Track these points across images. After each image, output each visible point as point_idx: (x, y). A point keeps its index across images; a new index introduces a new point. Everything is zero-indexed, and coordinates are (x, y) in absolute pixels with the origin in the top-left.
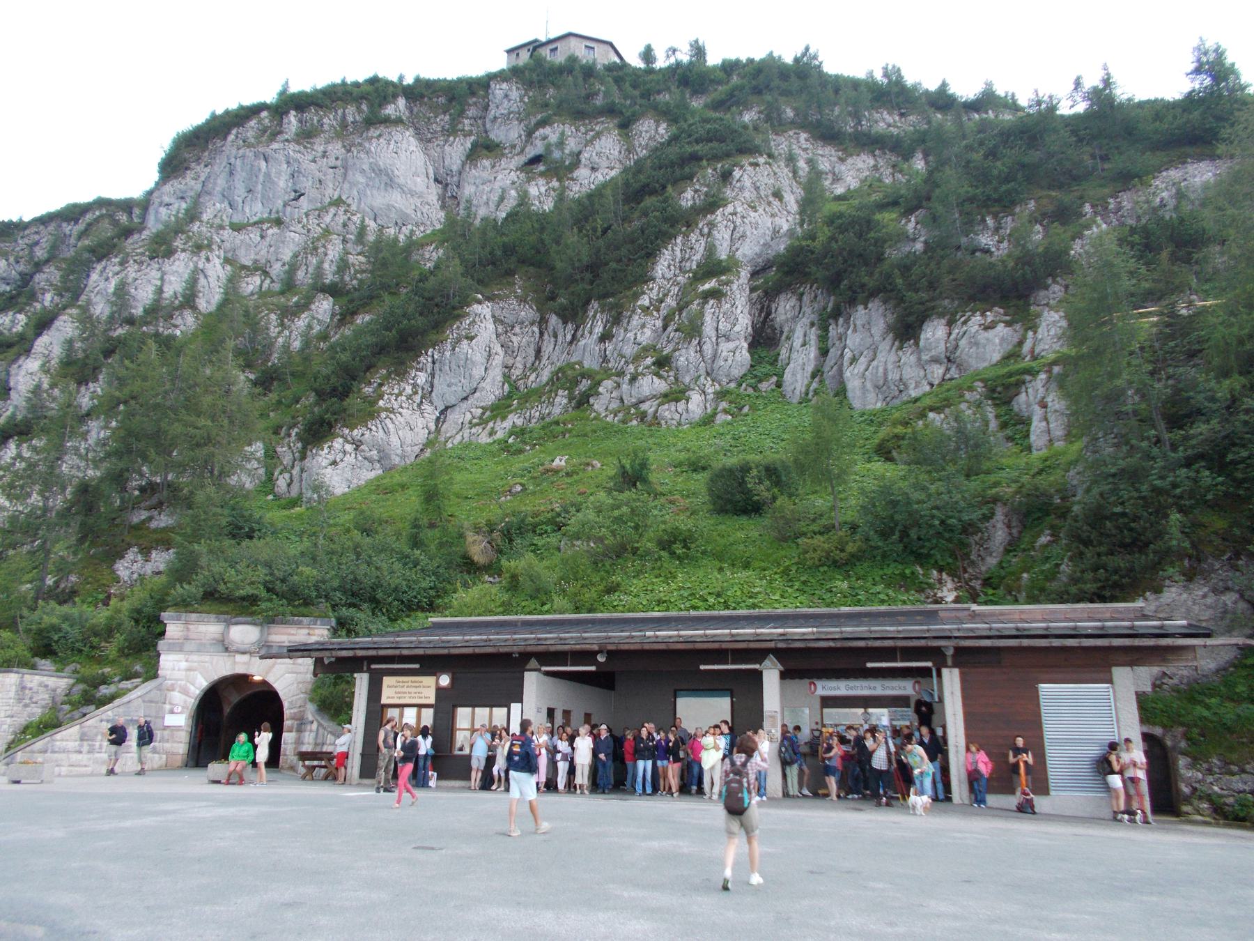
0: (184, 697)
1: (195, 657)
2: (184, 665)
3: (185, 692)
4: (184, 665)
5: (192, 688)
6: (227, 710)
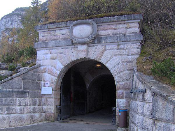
0: (51, 76)
1: (54, 51)
2: (49, 56)
3: (51, 73)
4: (49, 56)
5: (55, 70)
6: (88, 85)
